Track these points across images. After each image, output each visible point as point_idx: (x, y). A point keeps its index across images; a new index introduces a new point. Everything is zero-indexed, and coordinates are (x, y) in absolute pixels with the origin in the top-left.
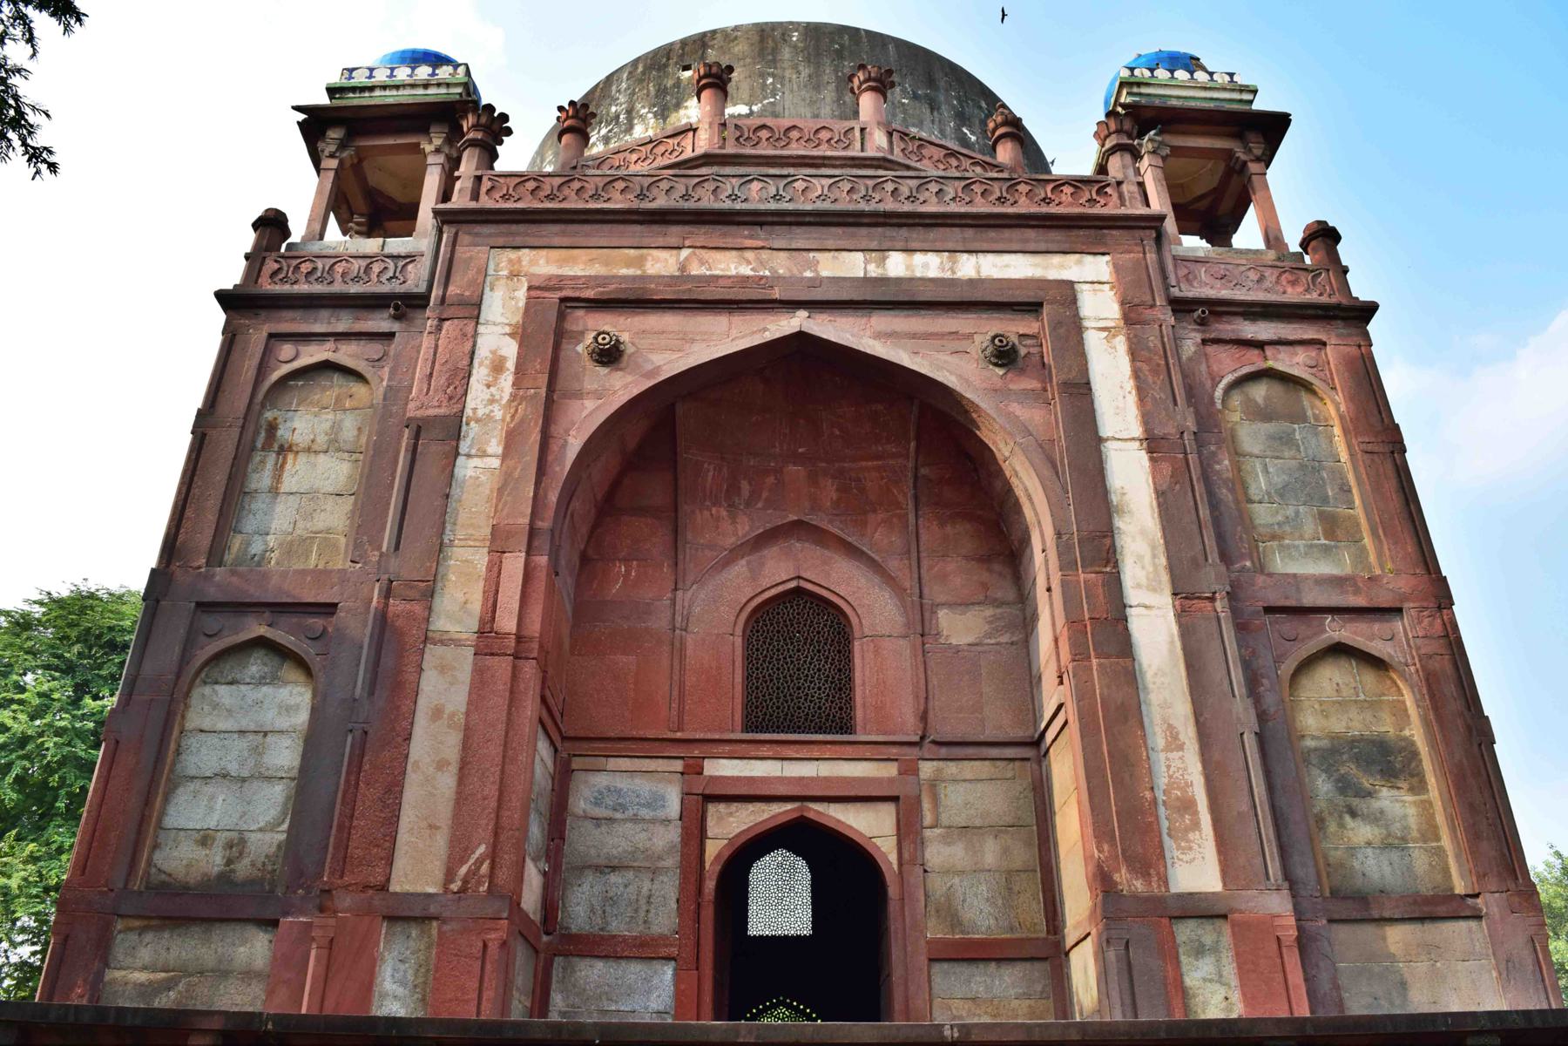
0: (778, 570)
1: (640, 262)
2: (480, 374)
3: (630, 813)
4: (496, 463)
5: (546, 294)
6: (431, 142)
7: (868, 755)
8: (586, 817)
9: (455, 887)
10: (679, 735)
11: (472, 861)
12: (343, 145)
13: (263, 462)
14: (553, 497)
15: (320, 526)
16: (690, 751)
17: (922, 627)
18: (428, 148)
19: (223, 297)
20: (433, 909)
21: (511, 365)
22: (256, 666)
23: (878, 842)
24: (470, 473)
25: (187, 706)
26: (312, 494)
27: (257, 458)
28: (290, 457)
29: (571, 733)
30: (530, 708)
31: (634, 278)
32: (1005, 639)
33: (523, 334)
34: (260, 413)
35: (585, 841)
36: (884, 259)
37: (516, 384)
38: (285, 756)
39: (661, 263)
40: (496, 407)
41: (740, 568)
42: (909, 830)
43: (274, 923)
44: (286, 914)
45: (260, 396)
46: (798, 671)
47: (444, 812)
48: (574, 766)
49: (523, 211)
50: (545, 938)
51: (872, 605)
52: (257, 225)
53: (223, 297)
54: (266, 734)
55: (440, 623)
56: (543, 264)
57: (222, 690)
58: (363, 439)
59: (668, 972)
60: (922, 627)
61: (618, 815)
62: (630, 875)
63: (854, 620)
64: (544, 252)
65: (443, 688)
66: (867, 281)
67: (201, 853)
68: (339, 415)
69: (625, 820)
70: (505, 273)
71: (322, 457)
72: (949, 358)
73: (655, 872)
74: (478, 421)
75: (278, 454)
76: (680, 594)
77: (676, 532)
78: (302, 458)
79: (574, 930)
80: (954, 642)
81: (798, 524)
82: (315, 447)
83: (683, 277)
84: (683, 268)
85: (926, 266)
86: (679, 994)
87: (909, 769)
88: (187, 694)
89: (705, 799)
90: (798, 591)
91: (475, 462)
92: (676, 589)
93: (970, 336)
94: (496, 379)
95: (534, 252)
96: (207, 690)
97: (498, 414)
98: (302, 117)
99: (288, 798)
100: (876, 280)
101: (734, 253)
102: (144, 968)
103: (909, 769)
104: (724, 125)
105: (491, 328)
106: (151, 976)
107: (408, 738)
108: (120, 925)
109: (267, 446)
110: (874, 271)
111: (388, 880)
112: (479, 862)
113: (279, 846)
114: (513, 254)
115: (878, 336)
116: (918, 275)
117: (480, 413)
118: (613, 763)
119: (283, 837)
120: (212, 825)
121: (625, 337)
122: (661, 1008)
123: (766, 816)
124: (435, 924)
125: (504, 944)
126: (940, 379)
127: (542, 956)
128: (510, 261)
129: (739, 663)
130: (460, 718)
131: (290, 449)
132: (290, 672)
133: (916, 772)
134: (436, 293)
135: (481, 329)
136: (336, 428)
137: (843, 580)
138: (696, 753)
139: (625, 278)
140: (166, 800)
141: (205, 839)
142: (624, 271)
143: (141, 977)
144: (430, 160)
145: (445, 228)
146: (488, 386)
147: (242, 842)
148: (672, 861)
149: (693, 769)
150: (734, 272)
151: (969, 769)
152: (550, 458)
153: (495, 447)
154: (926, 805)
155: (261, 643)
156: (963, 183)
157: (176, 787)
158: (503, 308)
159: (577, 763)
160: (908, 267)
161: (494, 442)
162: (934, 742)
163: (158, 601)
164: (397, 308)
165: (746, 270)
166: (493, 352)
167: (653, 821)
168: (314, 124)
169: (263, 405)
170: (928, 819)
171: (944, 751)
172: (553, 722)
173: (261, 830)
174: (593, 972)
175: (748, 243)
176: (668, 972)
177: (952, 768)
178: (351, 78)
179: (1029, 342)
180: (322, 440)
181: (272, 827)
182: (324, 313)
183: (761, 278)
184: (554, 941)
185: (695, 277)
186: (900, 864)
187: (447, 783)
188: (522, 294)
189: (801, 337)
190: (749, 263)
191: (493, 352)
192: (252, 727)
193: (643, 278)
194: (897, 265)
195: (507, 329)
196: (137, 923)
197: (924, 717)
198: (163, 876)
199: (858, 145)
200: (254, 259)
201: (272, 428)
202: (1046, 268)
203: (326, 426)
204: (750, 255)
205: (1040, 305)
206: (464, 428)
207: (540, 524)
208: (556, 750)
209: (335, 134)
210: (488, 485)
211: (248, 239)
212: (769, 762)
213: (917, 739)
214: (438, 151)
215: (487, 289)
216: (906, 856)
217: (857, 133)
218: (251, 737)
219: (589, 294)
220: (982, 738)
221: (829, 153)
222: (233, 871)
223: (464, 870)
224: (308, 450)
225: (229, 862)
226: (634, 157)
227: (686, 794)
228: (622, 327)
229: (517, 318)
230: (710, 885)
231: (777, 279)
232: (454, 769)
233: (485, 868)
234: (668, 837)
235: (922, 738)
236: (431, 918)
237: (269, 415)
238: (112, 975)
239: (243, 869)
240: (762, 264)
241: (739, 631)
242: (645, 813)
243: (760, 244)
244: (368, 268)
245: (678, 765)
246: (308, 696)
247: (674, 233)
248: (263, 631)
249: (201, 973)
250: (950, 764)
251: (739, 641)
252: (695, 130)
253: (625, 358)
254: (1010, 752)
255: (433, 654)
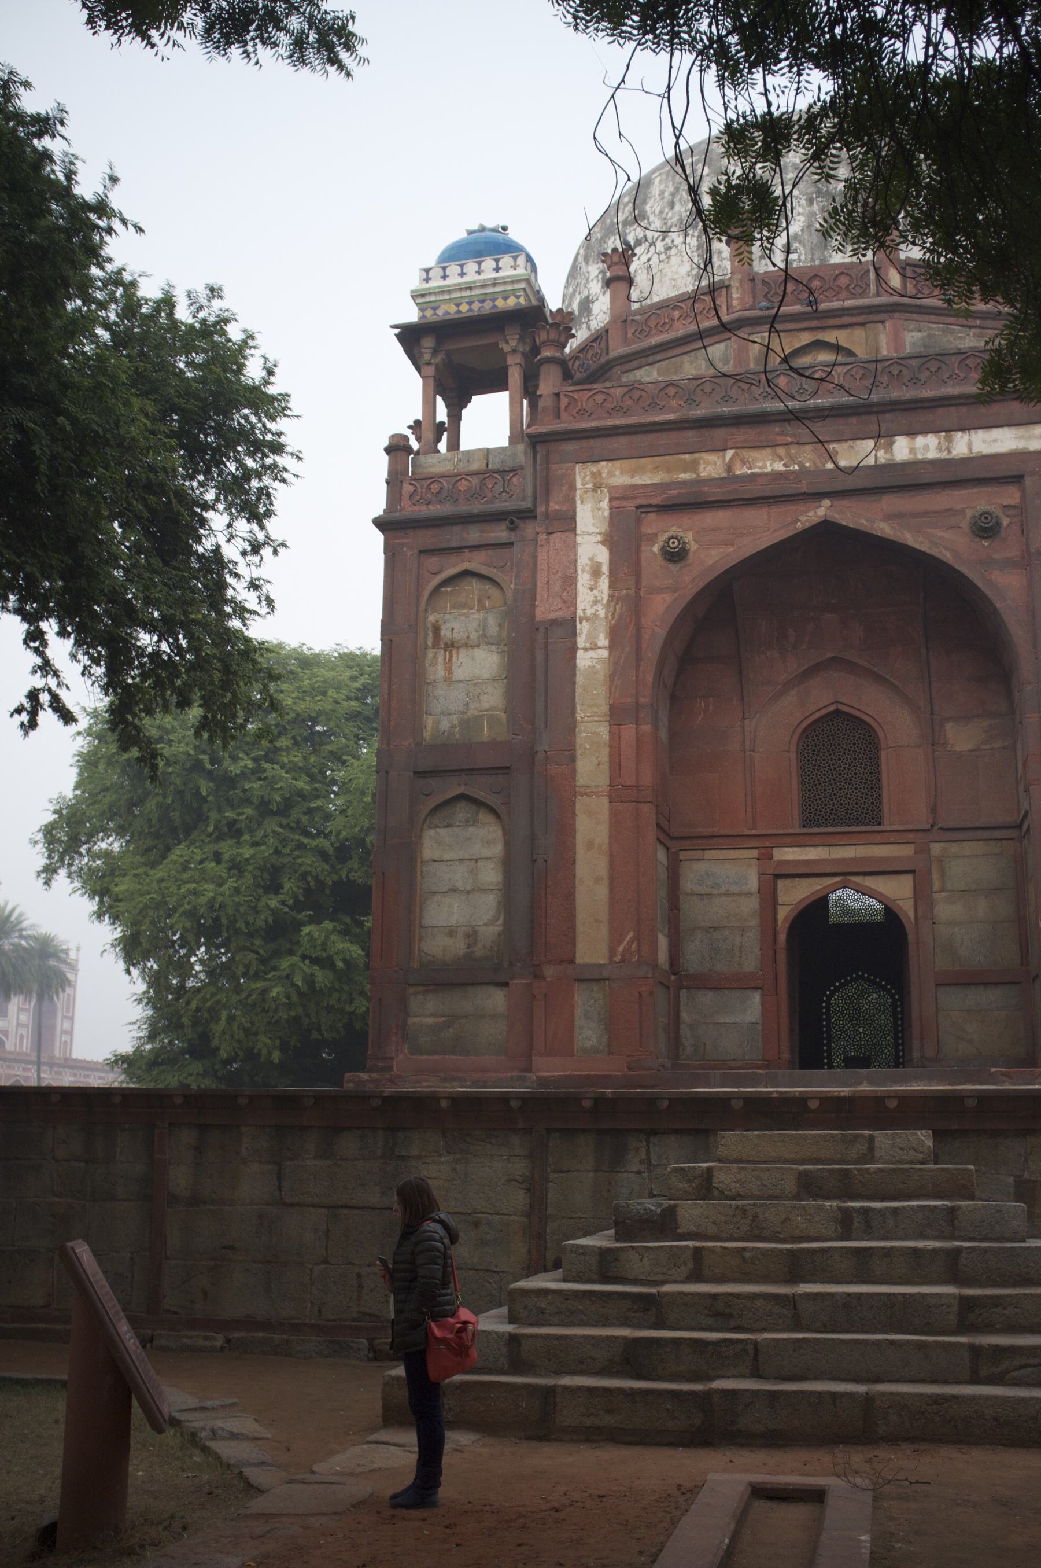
0: (819, 697)
1: (693, 466)
2: (583, 579)
3: (723, 890)
4: (605, 653)
5: (625, 504)
6: (507, 342)
7: (892, 840)
8: (692, 894)
9: (617, 959)
10: (753, 832)
11: (625, 943)
12: (435, 352)
13: (435, 657)
14: (649, 678)
15: (486, 705)
16: (765, 843)
17: (933, 740)
18: (506, 348)
19: (378, 523)
20: (605, 974)
21: (605, 569)
22: (462, 812)
23: (900, 903)
24: (588, 663)
25: (422, 845)
26: (475, 681)
27: (431, 653)
28: (454, 652)
29: (676, 835)
30: (651, 834)
31: (692, 482)
32: (998, 744)
33: (609, 540)
34: (426, 618)
35: (693, 911)
36: (892, 444)
37: (611, 586)
38: (491, 875)
39: (711, 466)
40: (599, 607)
41: (792, 697)
42: (922, 894)
43: (506, 984)
44: (512, 979)
45: (423, 604)
46: (839, 780)
47: (603, 913)
48: (681, 858)
49: (597, 429)
50: (673, 977)
51: (896, 722)
52: (388, 450)
53: (378, 523)
54: (476, 860)
55: (581, 780)
56: (618, 475)
57: (442, 831)
58: (504, 634)
59: (756, 997)
60: (933, 740)
61: (715, 892)
62: (727, 932)
63: (881, 735)
64: (618, 463)
65: (592, 825)
66: (877, 468)
67: (449, 941)
68: (481, 615)
69: (720, 895)
70: (590, 486)
71: (476, 650)
72: (942, 534)
73: (743, 930)
74: (588, 619)
75: (445, 650)
76: (747, 722)
77: (740, 673)
78: (462, 651)
79: (692, 971)
80: (958, 749)
81: (834, 659)
82: (470, 642)
83: (731, 478)
84: (729, 468)
85: (926, 447)
86: (764, 1012)
87: (923, 850)
88: (420, 837)
89: (775, 875)
90: (837, 712)
91: (591, 654)
92: (744, 718)
93: (963, 510)
94: (596, 582)
95: (610, 464)
96: (432, 832)
97: (602, 613)
98: (397, 331)
99: (499, 903)
100: (883, 466)
101: (769, 450)
102: (431, 1015)
103: (923, 850)
104: (753, 280)
105: (587, 538)
106: (436, 1020)
107: (574, 863)
108: (411, 990)
109: (436, 645)
110: (882, 456)
111: (574, 957)
112: (631, 942)
113: (499, 935)
114: (594, 468)
115: (888, 517)
116: (920, 457)
117: (589, 613)
118: (709, 854)
119: (500, 929)
120: (454, 923)
121: (689, 537)
122: (754, 1020)
123: (819, 887)
124: (607, 982)
125: (651, 993)
126: (937, 555)
127: (672, 991)
128: (593, 474)
129: (794, 774)
130: (605, 847)
131: (452, 645)
132: (485, 817)
133: (928, 850)
134: (541, 510)
135: (579, 539)
136: (484, 625)
137: (873, 703)
138: (767, 844)
139: (684, 483)
140: (421, 909)
141: (451, 932)
142: (683, 476)
143: (430, 1021)
144: (510, 360)
145: (538, 448)
146: (591, 589)
147: (475, 933)
148: (754, 922)
149: (766, 856)
150: (769, 469)
151: (968, 848)
152: (644, 646)
153: (603, 641)
154: (935, 876)
155: (462, 797)
156: (960, 357)
157: (426, 900)
158: (591, 518)
159: (683, 855)
160: (912, 450)
161: (602, 636)
162: (941, 828)
163: (387, 773)
164: (512, 522)
165: (779, 467)
166: (591, 559)
167: (740, 894)
168: (410, 337)
169: (426, 611)
170: (937, 885)
171: (949, 835)
172: (667, 836)
173: (485, 925)
174: (707, 998)
175: (780, 439)
176: (756, 997)
177: (954, 848)
178: (427, 280)
179: (1010, 512)
180: (474, 636)
181: (492, 922)
182: (457, 529)
183: (794, 472)
184: (679, 979)
185: (738, 476)
186: (916, 918)
187: (602, 891)
188: (605, 504)
189: (826, 527)
190: (781, 459)
191: (591, 559)
192: (467, 857)
193: (700, 482)
194: (902, 449)
195: (599, 538)
196: (421, 988)
197: (934, 810)
198: (429, 958)
199: (873, 288)
200: (394, 481)
201: (436, 629)
202: (1029, 438)
203: (474, 625)
204: (781, 451)
205: (1022, 477)
206: (579, 626)
207: (642, 700)
208: (668, 849)
209: (428, 343)
210: (602, 671)
211: (382, 464)
212: (820, 849)
213: (928, 827)
214: (514, 351)
215: (578, 503)
216: (920, 913)
217: (872, 275)
218: (468, 863)
219: (656, 501)
220: (978, 824)
221: (849, 303)
222: (473, 952)
223: (621, 948)
224: (466, 645)
225: (469, 946)
226: (677, 314)
227: (761, 874)
228: (684, 529)
229: (604, 527)
230: (782, 937)
231: (804, 471)
232: (605, 884)
233: (634, 947)
234: (751, 905)
235: (932, 826)
236: (604, 980)
237: (431, 618)
238: (411, 1021)
239: (479, 951)
240: (792, 459)
241: (793, 748)
242: (734, 889)
243: (790, 439)
244: (483, 483)
245: (755, 853)
246: (500, 832)
247: (720, 433)
248: (462, 789)
249: (467, 1017)
250: (953, 844)
251: (793, 756)
252: (728, 287)
253: (691, 555)
254: (998, 834)
255: (581, 803)
